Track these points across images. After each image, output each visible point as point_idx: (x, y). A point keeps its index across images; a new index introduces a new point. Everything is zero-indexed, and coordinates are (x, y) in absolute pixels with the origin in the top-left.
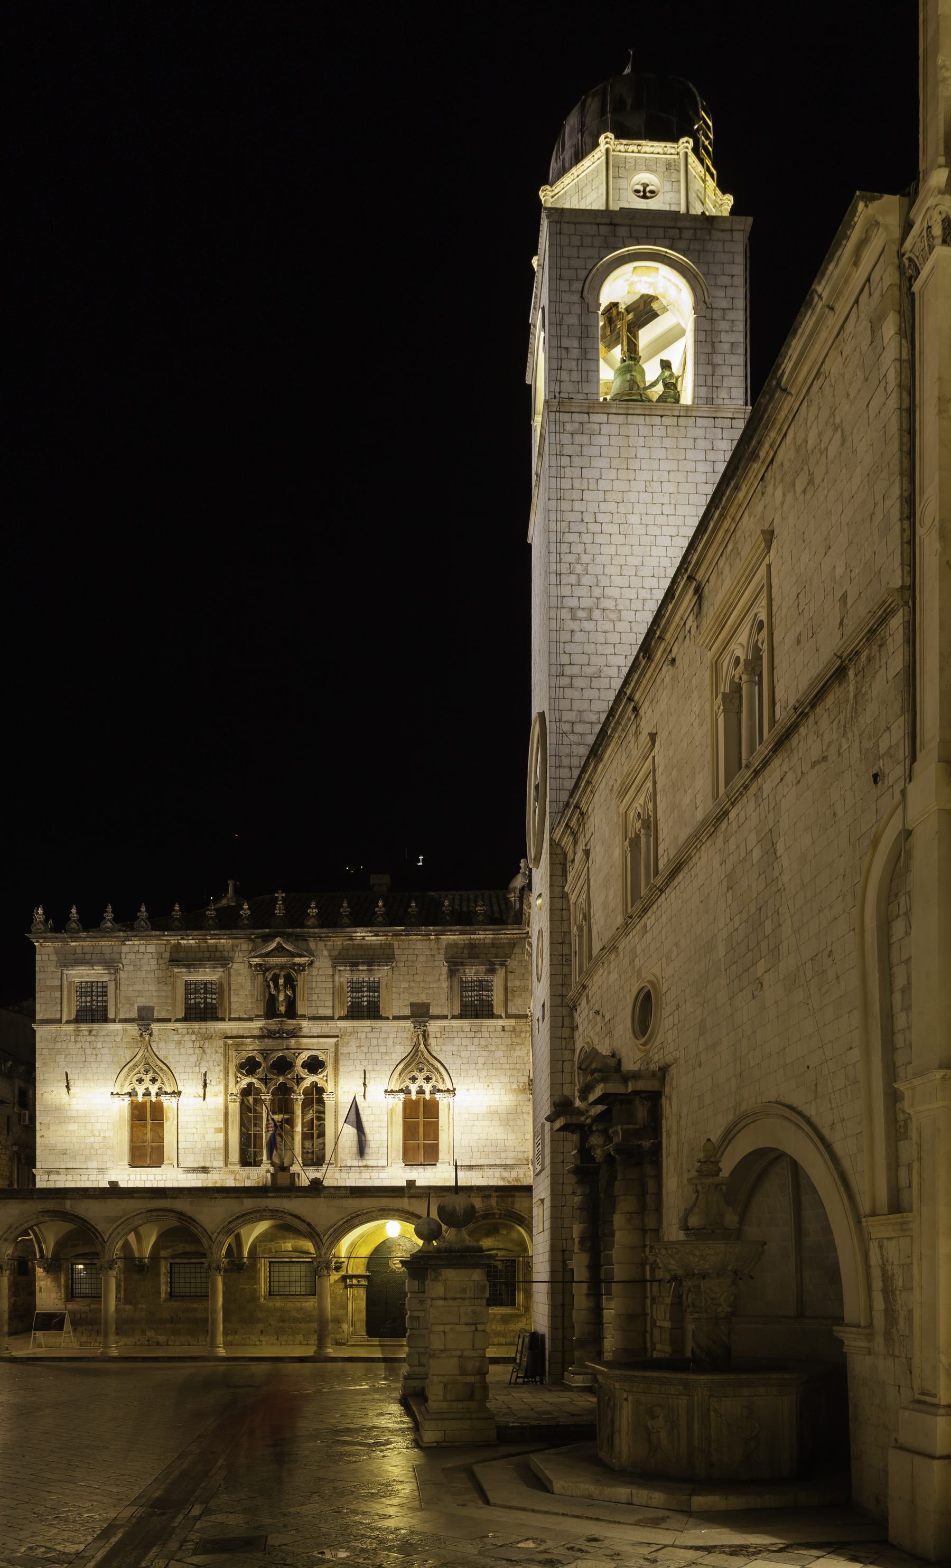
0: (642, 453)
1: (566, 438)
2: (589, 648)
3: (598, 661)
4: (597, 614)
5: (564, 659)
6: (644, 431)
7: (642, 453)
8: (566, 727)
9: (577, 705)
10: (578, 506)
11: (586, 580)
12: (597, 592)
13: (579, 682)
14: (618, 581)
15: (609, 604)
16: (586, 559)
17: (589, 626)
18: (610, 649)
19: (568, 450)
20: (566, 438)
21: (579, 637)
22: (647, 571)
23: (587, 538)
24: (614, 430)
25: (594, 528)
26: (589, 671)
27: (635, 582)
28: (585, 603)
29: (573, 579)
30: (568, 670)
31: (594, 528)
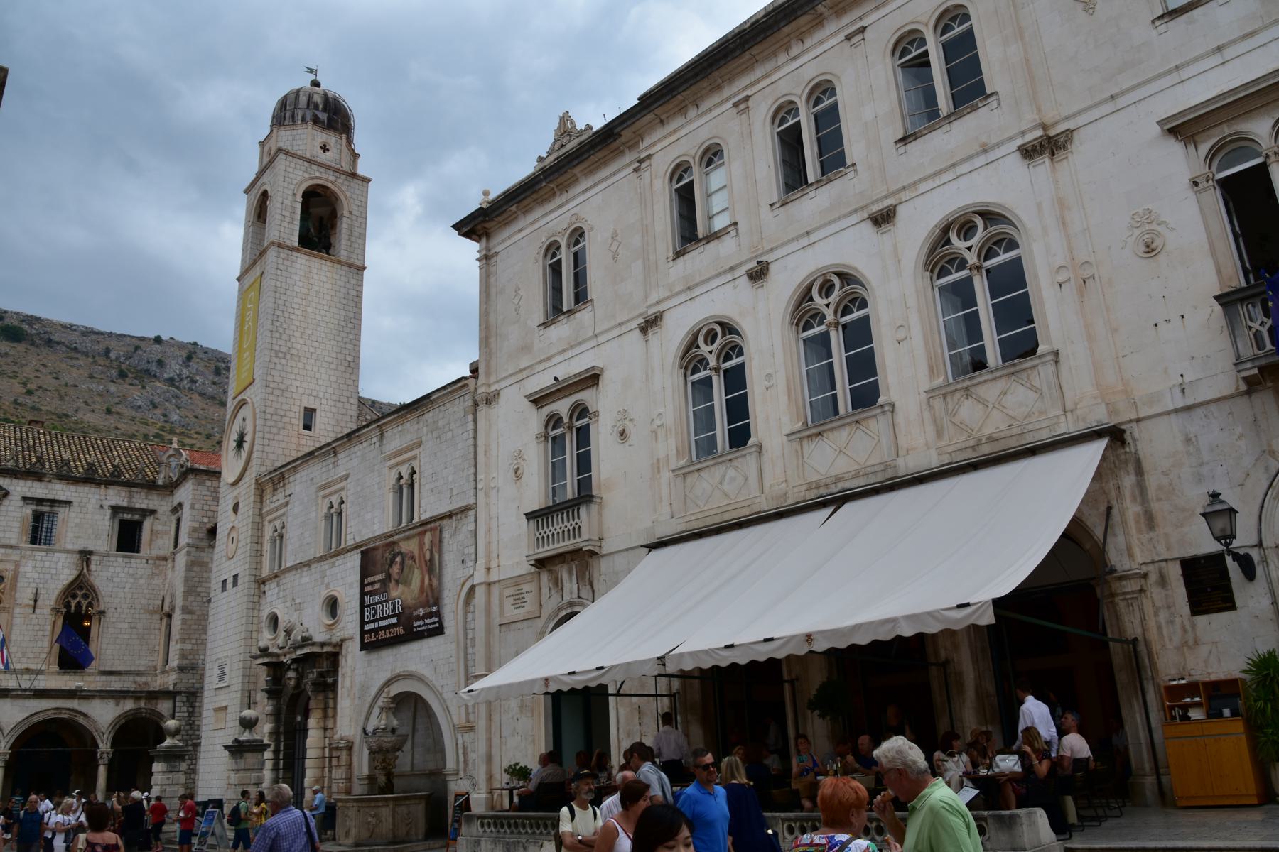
0: (316, 277)
1: (280, 261)
2: (283, 374)
3: (287, 382)
4: (288, 356)
5: (270, 378)
6: (318, 266)
7: (316, 277)
8: (268, 416)
9: (275, 405)
10: (283, 297)
11: (284, 337)
12: (289, 344)
13: (277, 392)
14: (301, 341)
15: (294, 352)
16: (285, 326)
17: (283, 361)
18: (293, 377)
19: (281, 267)
20: (280, 261)
21: (279, 367)
22: (313, 338)
23: (286, 315)
24: (303, 262)
25: (290, 310)
26: (282, 386)
27: (308, 342)
28: (283, 349)
29: (277, 335)
30: (272, 385)
31: (290, 310)
